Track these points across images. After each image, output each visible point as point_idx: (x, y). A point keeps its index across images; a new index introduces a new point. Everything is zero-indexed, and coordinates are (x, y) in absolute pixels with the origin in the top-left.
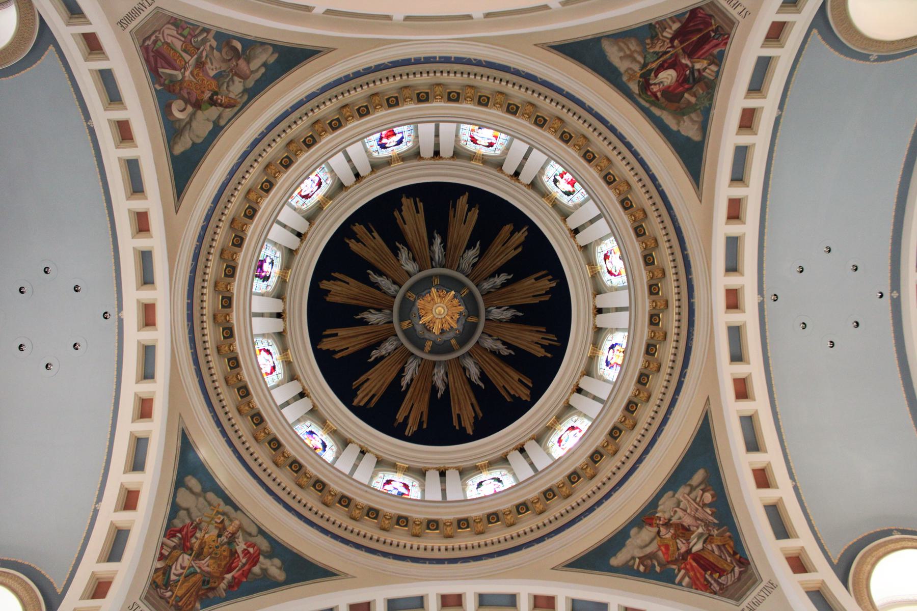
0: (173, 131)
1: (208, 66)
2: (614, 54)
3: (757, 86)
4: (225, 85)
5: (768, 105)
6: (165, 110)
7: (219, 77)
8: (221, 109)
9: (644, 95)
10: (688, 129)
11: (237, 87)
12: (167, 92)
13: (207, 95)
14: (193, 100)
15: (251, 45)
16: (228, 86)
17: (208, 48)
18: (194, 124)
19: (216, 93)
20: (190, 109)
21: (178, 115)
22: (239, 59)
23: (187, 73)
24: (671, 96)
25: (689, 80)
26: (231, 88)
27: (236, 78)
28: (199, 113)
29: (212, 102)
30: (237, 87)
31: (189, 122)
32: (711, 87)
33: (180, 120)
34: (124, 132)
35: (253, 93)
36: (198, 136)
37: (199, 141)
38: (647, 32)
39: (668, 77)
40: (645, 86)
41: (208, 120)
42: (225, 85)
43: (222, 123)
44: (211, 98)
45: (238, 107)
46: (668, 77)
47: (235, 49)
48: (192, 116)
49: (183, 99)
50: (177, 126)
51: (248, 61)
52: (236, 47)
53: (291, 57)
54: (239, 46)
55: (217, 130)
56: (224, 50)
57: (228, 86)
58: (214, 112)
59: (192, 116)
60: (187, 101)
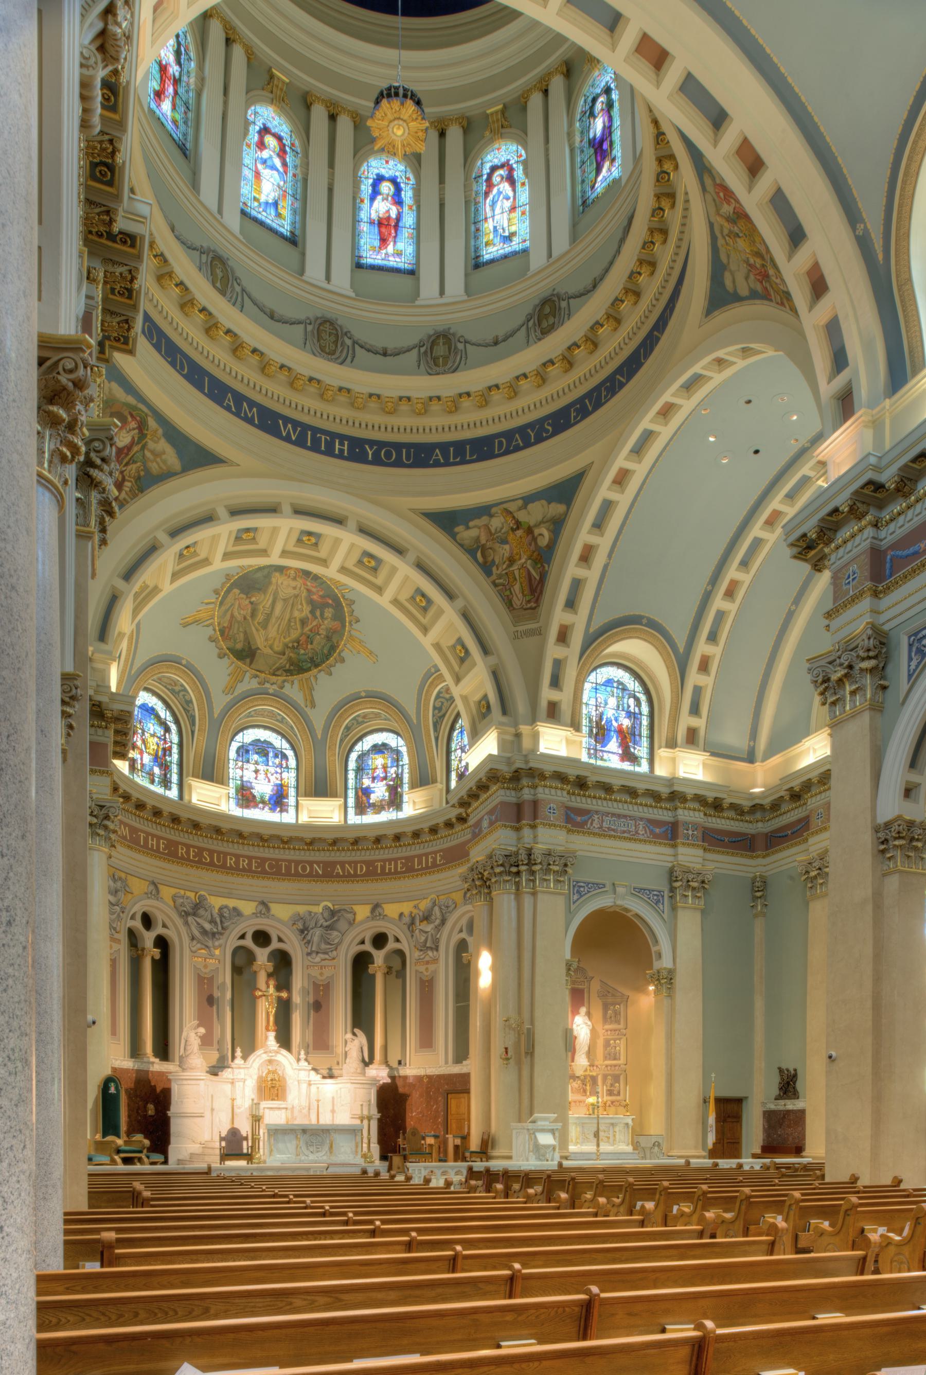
0: (557, 524)
1: (507, 555)
4: (503, 531)
7: (504, 541)
8: (515, 515)
13: (519, 533)
14: (530, 537)
15: (471, 552)
16: (502, 529)
17: (500, 569)
18: (540, 518)
19: (513, 530)
20: (537, 532)
21: (546, 534)
22: (483, 545)
23: (523, 560)
26: (500, 525)
27: (493, 531)
28: (532, 523)
29: (518, 525)
31: (542, 522)
33: (548, 529)
36: (543, 506)
37: (544, 502)
41: (529, 513)
42: (503, 531)
43: (520, 503)
44: (518, 528)
47: (483, 555)
48: (538, 525)
49: (536, 543)
50: (551, 527)
51: (477, 539)
54: (479, 555)
56: (490, 559)
57: (502, 529)
58: (522, 516)
59: (538, 525)
60: (535, 539)
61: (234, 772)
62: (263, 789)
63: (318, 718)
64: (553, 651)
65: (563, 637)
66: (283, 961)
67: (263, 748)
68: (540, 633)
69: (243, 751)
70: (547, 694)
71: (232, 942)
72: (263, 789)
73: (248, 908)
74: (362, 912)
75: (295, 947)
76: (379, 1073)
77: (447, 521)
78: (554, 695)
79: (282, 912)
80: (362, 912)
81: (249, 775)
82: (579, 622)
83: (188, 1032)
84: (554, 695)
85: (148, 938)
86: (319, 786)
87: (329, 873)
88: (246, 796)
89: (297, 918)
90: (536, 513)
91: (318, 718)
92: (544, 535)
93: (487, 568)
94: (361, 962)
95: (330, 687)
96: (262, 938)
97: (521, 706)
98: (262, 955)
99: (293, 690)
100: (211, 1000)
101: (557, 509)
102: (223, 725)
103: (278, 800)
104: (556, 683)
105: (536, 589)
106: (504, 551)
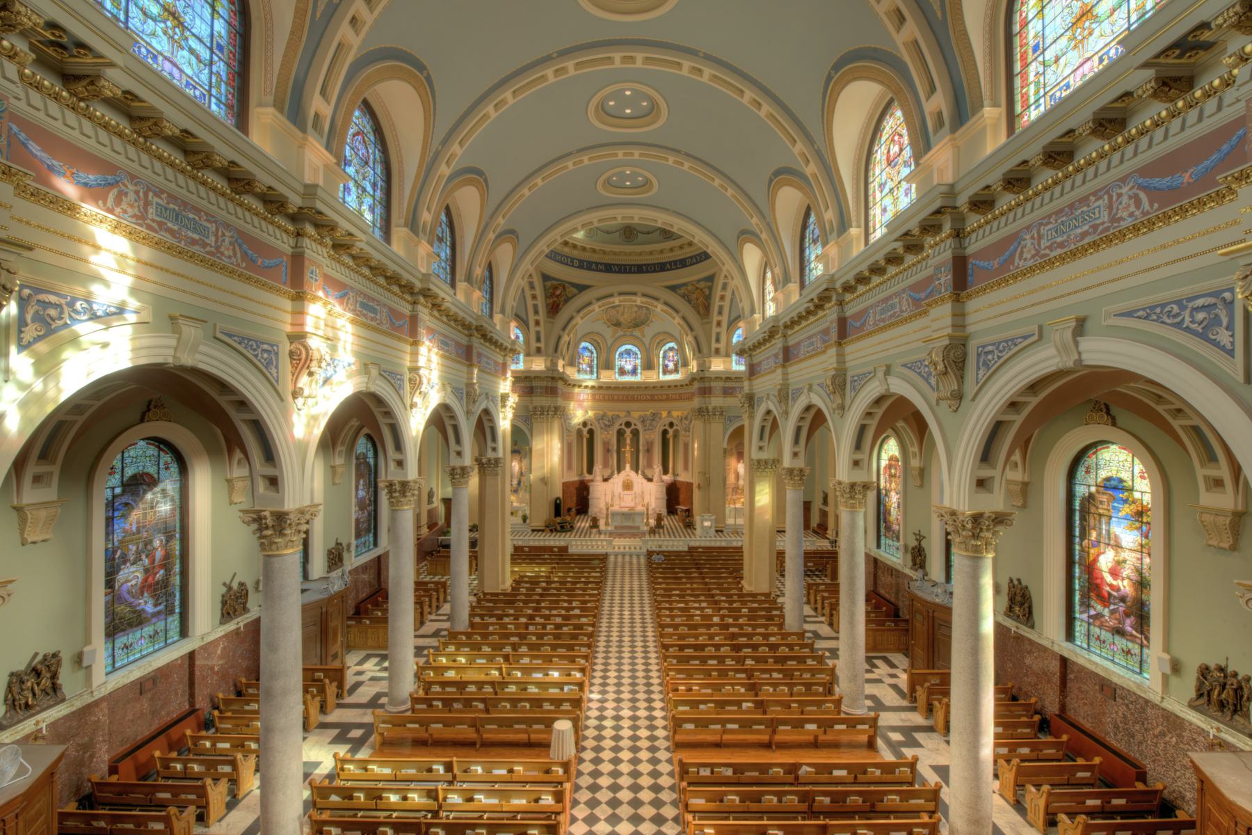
0: (710, 288)
2: (574, 290)
3: (535, 306)
5: (530, 303)
6: (710, 295)
9: (563, 285)
10: (549, 284)
11: (690, 288)
12: (708, 298)
15: (683, 297)
24: (556, 288)
25: (553, 295)
30: (690, 288)
32: (547, 297)
34: (722, 298)
35: (685, 285)
38: (566, 301)
39: (558, 292)
40: (564, 288)
45: (691, 283)
46: (558, 292)
52: (687, 298)
53: (673, 288)
55: (699, 281)
61: (618, 363)
62: (629, 367)
63: (647, 341)
64: (715, 330)
65: (719, 324)
66: (636, 433)
67: (628, 352)
68: (710, 323)
69: (621, 354)
70: (714, 345)
71: (617, 427)
72: (629, 367)
73: (622, 414)
74: (664, 414)
75: (640, 427)
76: (668, 478)
77: (673, 288)
78: (718, 346)
79: (636, 415)
80: (664, 414)
81: (623, 363)
82: (725, 319)
83: (598, 468)
84: (718, 346)
85: (585, 431)
86: (649, 365)
87: (652, 399)
88: (622, 372)
89: (641, 417)
90: (702, 285)
91: (647, 341)
92: (707, 292)
93: (689, 301)
94: (665, 432)
95: (649, 331)
96: (628, 424)
97: (705, 350)
98: (628, 431)
99: (637, 332)
100: (608, 451)
101: (709, 284)
102: (611, 349)
103: (634, 372)
104: (718, 340)
105: (707, 308)
106: (694, 296)
